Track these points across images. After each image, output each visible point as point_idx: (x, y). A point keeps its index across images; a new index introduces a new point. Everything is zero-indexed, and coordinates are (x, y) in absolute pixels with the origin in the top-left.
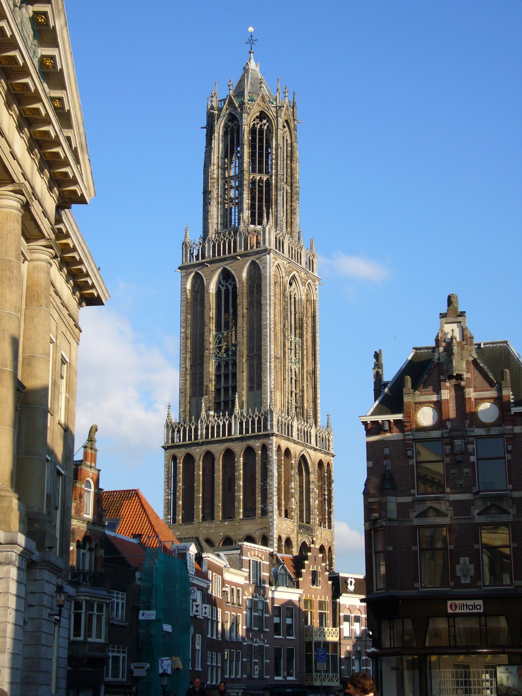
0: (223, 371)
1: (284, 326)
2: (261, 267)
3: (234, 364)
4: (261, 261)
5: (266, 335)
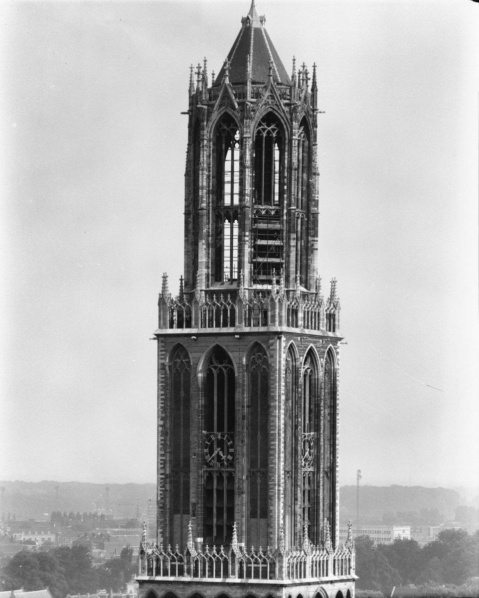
3: (231, 478)
5: (275, 449)
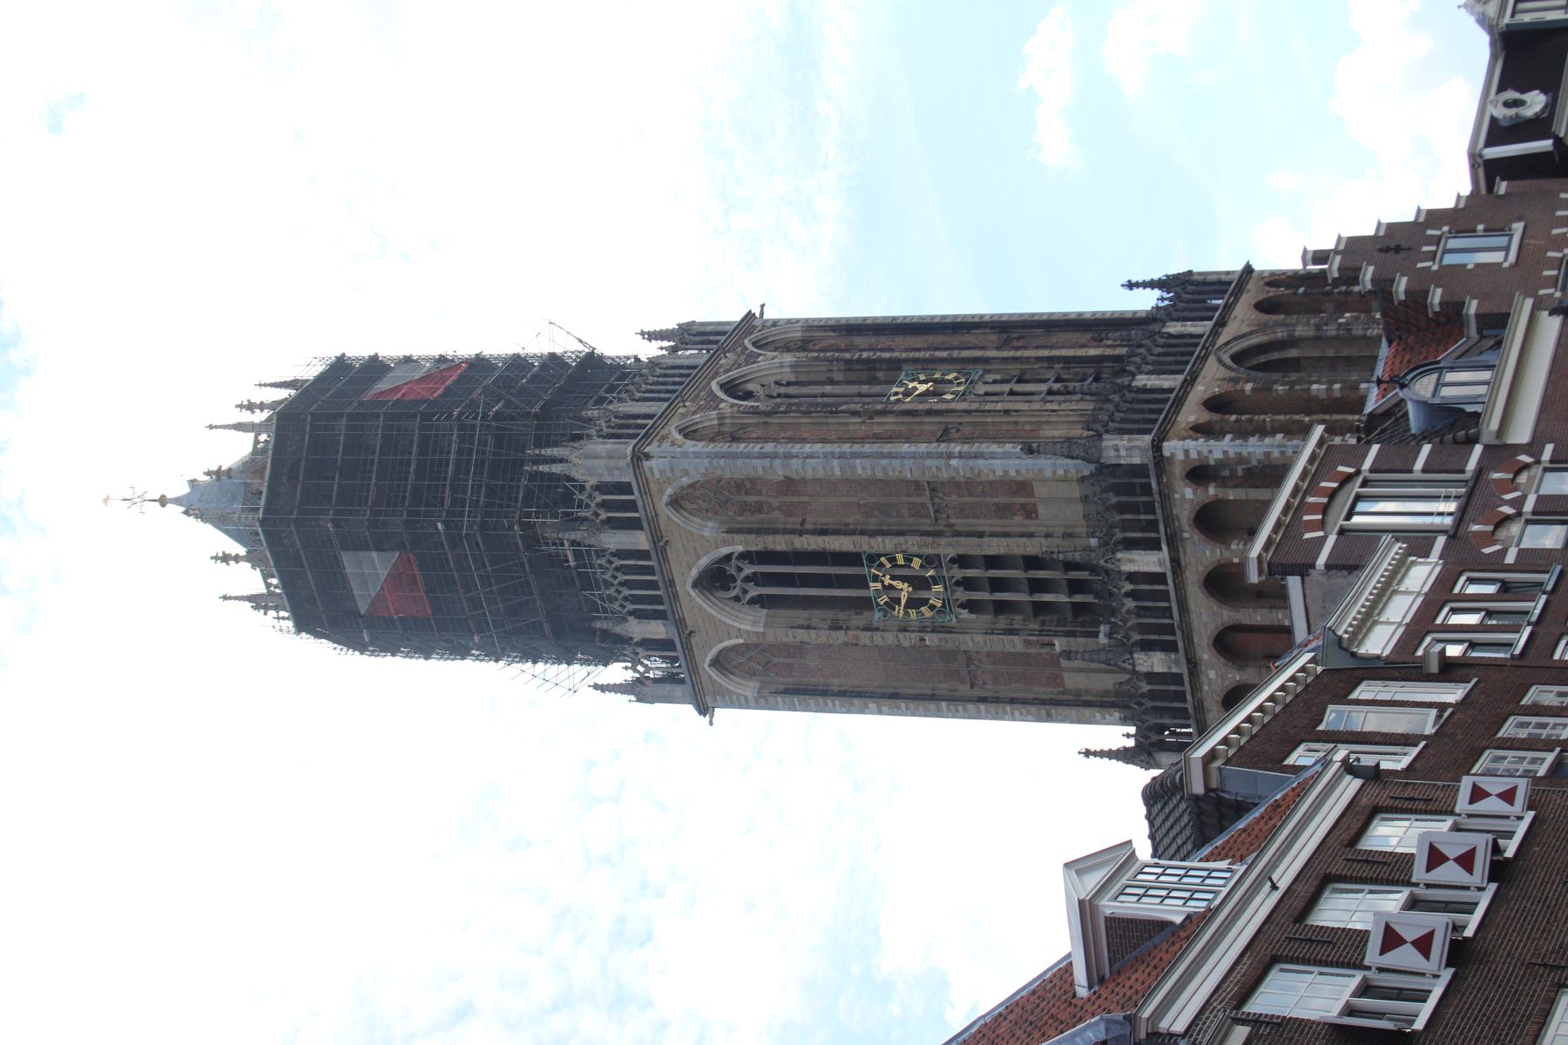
0: (984, 596)
1: (854, 413)
2: (685, 481)
4: (668, 481)
